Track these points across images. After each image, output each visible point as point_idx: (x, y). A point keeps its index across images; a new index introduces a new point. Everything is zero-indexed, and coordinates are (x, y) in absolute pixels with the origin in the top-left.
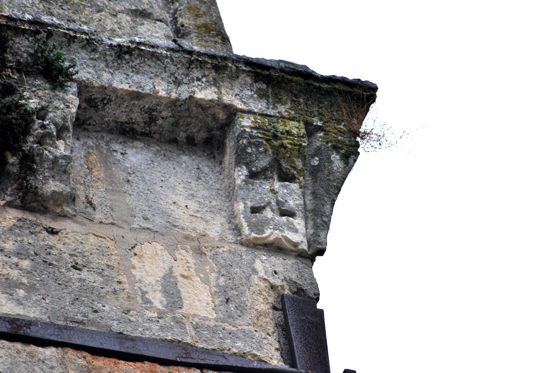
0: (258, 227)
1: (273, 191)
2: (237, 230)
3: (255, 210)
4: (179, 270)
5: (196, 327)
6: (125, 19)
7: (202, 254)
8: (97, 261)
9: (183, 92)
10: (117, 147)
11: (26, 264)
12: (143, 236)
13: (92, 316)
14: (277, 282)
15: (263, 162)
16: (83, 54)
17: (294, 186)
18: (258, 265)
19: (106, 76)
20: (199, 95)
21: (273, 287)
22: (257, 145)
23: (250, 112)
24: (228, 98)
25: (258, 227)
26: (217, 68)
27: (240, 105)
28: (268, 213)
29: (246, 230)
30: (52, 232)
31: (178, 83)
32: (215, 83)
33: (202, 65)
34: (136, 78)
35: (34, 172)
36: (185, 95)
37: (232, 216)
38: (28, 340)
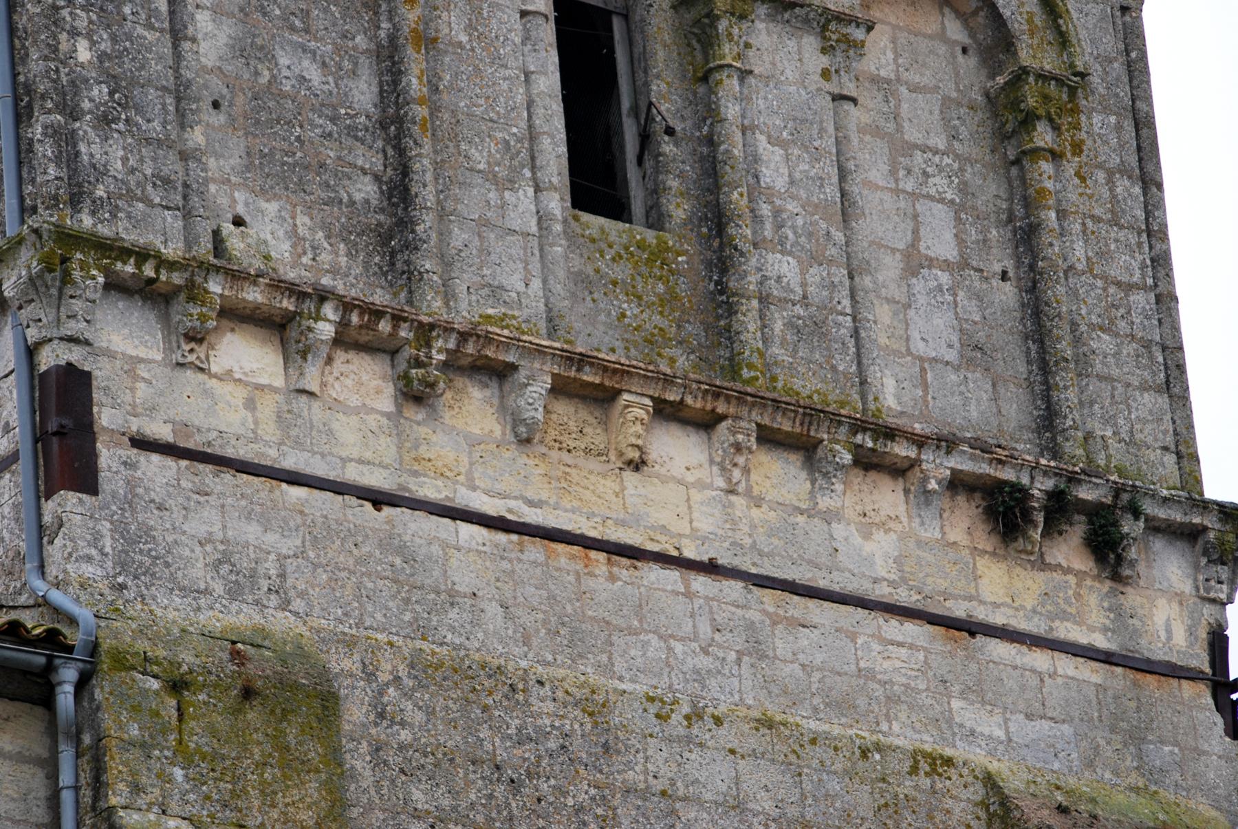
0: (1208, 590)
1: (1217, 572)
2: (1197, 589)
3: (1207, 580)
4: (1172, 616)
5: (1178, 652)
6: (1159, 451)
7: (1182, 604)
8: (1140, 612)
9: (1187, 519)
10: (1151, 538)
11: (1112, 616)
12: (1159, 594)
13: (1137, 647)
14: (1212, 621)
15: (1215, 557)
16: (1149, 500)
17: (1226, 568)
18: (1205, 611)
19: (1156, 510)
20: (1194, 521)
21: (1209, 624)
22: (1215, 548)
23: (1214, 529)
24: (1205, 523)
25: (1208, 590)
26: (1205, 508)
27: (1210, 526)
28: (1213, 583)
29: (1202, 591)
30: (1122, 593)
31: (1186, 514)
32: (1202, 514)
33: (1198, 506)
34: (1169, 511)
35: (1120, 565)
36: (1188, 521)
37: (1196, 580)
38: (1111, 663)
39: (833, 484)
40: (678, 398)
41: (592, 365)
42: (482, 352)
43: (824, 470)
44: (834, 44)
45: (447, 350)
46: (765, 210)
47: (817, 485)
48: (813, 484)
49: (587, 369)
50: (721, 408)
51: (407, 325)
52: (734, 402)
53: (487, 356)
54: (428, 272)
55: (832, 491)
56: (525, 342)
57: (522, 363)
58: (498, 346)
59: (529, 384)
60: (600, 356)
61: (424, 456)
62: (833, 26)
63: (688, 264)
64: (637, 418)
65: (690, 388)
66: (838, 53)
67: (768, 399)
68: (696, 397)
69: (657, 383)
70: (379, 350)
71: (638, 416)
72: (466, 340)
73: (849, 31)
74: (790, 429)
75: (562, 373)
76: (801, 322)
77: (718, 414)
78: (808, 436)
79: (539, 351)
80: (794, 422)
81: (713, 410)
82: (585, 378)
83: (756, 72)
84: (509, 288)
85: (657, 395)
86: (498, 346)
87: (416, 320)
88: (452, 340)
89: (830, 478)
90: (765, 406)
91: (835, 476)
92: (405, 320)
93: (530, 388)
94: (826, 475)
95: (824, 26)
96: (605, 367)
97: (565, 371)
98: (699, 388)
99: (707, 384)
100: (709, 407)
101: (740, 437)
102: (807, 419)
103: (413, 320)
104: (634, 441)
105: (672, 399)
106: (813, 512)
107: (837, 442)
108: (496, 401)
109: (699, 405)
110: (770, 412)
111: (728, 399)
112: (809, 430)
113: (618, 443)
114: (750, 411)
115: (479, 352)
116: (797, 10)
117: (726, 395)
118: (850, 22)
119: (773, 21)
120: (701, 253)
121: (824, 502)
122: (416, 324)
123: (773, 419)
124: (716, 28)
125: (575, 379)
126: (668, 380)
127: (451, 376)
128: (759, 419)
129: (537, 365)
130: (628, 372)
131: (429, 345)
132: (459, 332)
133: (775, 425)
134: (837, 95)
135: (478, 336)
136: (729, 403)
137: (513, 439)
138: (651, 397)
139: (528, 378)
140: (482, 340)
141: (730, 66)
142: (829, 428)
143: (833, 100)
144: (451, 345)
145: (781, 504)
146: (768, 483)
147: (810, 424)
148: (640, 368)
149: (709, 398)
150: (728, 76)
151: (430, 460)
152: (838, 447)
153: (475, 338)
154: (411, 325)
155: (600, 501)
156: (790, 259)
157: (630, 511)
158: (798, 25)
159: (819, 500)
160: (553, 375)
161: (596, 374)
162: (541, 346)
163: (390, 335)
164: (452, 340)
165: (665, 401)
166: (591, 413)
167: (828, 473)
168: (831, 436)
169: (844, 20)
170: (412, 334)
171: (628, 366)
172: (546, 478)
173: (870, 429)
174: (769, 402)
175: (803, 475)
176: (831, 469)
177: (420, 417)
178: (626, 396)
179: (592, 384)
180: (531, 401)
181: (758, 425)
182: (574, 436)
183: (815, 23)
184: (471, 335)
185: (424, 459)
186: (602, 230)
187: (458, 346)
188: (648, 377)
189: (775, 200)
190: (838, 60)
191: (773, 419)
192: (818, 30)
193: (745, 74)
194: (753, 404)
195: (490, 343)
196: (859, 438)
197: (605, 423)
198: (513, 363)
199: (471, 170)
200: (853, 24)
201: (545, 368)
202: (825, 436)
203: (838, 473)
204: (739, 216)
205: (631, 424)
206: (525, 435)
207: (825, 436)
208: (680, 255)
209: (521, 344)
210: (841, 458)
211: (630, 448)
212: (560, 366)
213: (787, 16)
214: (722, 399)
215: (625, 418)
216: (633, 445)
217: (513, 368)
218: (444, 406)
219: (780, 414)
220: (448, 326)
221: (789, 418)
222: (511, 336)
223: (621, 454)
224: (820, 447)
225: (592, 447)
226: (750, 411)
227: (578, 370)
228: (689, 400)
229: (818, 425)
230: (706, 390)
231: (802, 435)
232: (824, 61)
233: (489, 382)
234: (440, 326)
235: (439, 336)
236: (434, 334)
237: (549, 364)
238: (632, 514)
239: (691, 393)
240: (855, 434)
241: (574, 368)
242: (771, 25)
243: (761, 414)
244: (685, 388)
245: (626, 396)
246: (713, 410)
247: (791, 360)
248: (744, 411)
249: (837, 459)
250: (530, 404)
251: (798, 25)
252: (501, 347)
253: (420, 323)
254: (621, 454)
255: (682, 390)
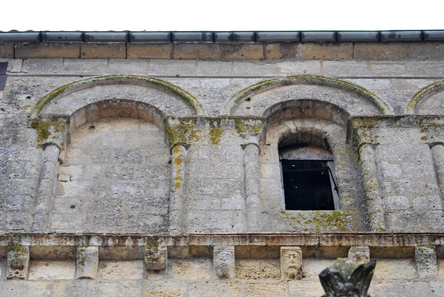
39: (427, 265)
40: (316, 244)
41: (258, 237)
42: (190, 244)
43: (419, 260)
44: (426, 127)
45: (168, 247)
46: (386, 184)
47: (419, 269)
48: (416, 269)
49: (256, 240)
50: (345, 243)
51: (141, 239)
52: (352, 239)
53: (193, 245)
54: (172, 230)
55: (428, 269)
56: (214, 235)
57: (215, 244)
58: (198, 240)
59: (219, 252)
60: (262, 233)
61: (158, 291)
62: (424, 121)
63: (352, 218)
64: (290, 255)
65: (322, 237)
66: (430, 130)
67: (373, 234)
68: (327, 241)
69: (301, 239)
70: (137, 259)
71: (290, 253)
72: (179, 240)
73: (434, 122)
74: (392, 246)
75: (241, 244)
76: (409, 216)
77: (345, 247)
78: (404, 246)
79: (224, 237)
80: (393, 242)
81: (340, 246)
82: (256, 244)
83: (381, 143)
84: (222, 228)
85: (303, 244)
86: (198, 240)
87: (145, 236)
88: (170, 242)
89: (424, 263)
90: (371, 237)
91: (427, 262)
92: (140, 238)
93: (220, 253)
94: (421, 262)
95: (420, 123)
96: (266, 237)
97: (242, 243)
98: (328, 236)
99: (332, 234)
100: (337, 244)
101: (358, 253)
102: (401, 239)
103: (144, 237)
104: (291, 265)
105: (312, 244)
106: (417, 279)
107: (424, 246)
108: (208, 267)
109: (330, 244)
110: (376, 240)
111: (347, 238)
112: (404, 244)
113: (284, 270)
114: (363, 242)
115: (188, 244)
116: (402, 119)
117: (345, 236)
118: (434, 118)
119: (392, 127)
120: (360, 213)
121: (423, 274)
122: (146, 238)
123: (380, 243)
124: (357, 134)
125: (250, 246)
126: (307, 236)
127: (180, 262)
128: (370, 244)
129: (225, 243)
130: (281, 237)
131: (156, 246)
132: (173, 237)
133: (381, 245)
134: (431, 144)
135: (185, 237)
136: (349, 240)
137: (217, 278)
138: (300, 246)
139: (219, 249)
140: (188, 238)
141: (365, 143)
142: (416, 240)
143: (431, 147)
144: (171, 243)
145: (395, 279)
146: (387, 273)
147: (404, 241)
148: (289, 234)
149: (336, 240)
150: (365, 147)
151: (161, 292)
152: (423, 248)
153: (183, 238)
154: (144, 239)
155: (272, 293)
156: (402, 197)
157: (292, 294)
158: (406, 126)
159: (421, 274)
160: (236, 247)
161: (262, 242)
162: (225, 234)
163: (134, 246)
164: (170, 242)
165: (309, 247)
166: (270, 263)
167: (422, 260)
168: (419, 244)
169: (430, 118)
170: (146, 243)
171: (280, 234)
172: (237, 289)
173: (442, 236)
174: (374, 235)
175: (411, 267)
176: (423, 258)
177: (158, 278)
178: (282, 248)
179: (261, 247)
180: (221, 258)
181: (369, 246)
182: (258, 273)
183: (415, 123)
184: (181, 237)
185: (158, 292)
186: (300, 215)
187: (175, 243)
188: (294, 237)
189: (393, 180)
190: (431, 133)
191: (380, 243)
192: (418, 126)
193: (375, 146)
194: (364, 239)
195: (193, 239)
196: (437, 242)
197: (278, 266)
198: (210, 245)
199: (204, 194)
200: (436, 118)
201: (229, 244)
202: (415, 245)
203: (429, 260)
204: (370, 188)
205: (288, 258)
206: (221, 273)
207: (415, 245)
208: (348, 216)
209: (212, 236)
210: (427, 252)
211: (290, 269)
212: (239, 242)
213: (398, 123)
214: (344, 239)
215: (284, 257)
216: (290, 267)
217: (211, 248)
218: (175, 273)
219: (383, 239)
220: (166, 236)
221: (390, 241)
222: (206, 233)
223: (287, 274)
224: (416, 251)
225: (270, 275)
226: (363, 242)
227: (251, 242)
228: (323, 243)
229: (409, 240)
230: (332, 236)
231: (401, 247)
232: (423, 134)
233: (204, 261)
234: (161, 237)
235: (162, 241)
236: (159, 241)
237: (232, 242)
238: (293, 295)
239: (324, 240)
240: (435, 240)
241: (248, 241)
242: (391, 129)
243: (371, 242)
244: (319, 238)
245: (282, 248)
246: (340, 246)
247: (402, 229)
248: (360, 242)
249: (424, 252)
250: (222, 259)
251: (406, 126)
252: (201, 240)
253: (149, 237)
254: (287, 274)
255: (318, 239)
